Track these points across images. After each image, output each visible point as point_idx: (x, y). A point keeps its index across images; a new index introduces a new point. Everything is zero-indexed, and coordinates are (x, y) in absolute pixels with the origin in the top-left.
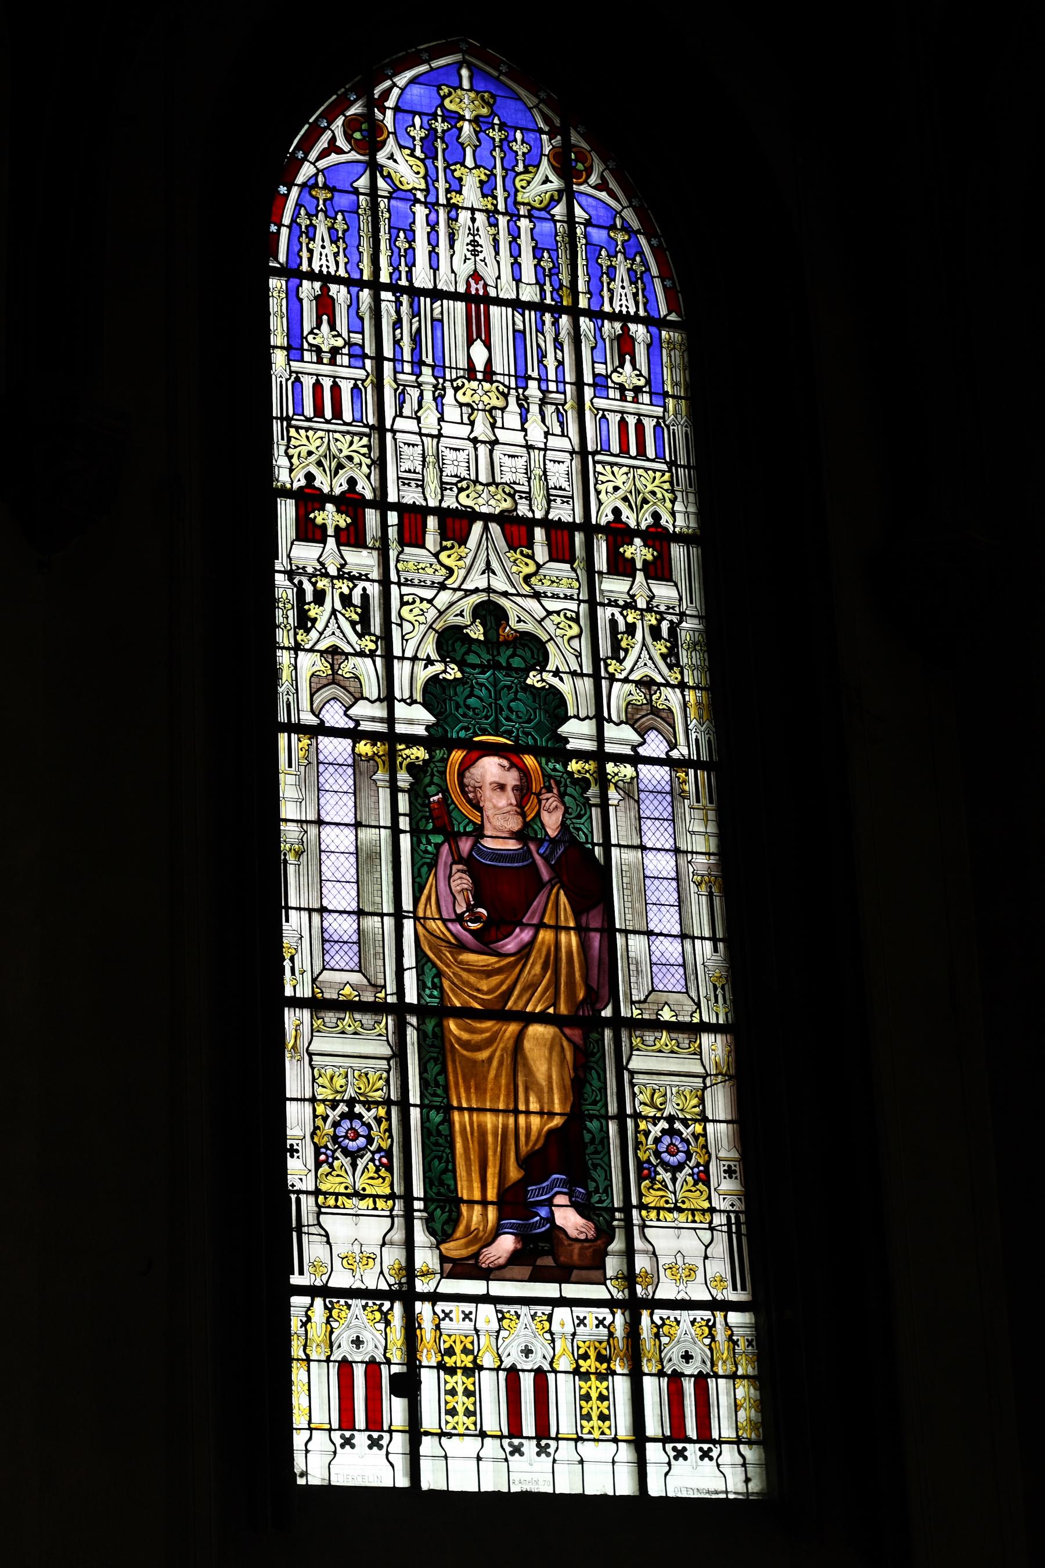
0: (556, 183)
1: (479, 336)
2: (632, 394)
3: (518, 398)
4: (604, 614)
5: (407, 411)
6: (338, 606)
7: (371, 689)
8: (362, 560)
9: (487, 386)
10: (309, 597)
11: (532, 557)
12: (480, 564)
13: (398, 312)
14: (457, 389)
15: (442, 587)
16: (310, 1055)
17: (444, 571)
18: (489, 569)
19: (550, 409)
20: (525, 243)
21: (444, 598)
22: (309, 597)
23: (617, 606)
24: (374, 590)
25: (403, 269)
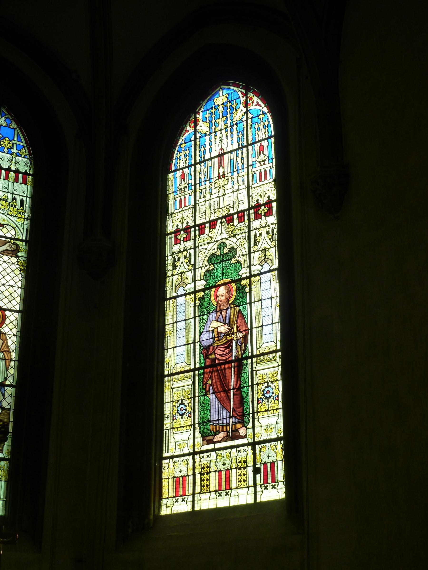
0: (244, 110)
1: (221, 166)
2: (263, 163)
3: (231, 179)
4: (252, 233)
5: (202, 196)
6: (183, 259)
7: (191, 280)
8: (190, 244)
9: (223, 179)
10: (177, 260)
11: (233, 225)
12: (220, 232)
13: (200, 169)
14: (215, 184)
15: (209, 243)
16: (172, 389)
17: (210, 238)
18: (222, 233)
19: (239, 179)
20: (235, 133)
21: (211, 245)
22: (177, 260)
23: (257, 229)
24: (192, 251)
25: (203, 156)
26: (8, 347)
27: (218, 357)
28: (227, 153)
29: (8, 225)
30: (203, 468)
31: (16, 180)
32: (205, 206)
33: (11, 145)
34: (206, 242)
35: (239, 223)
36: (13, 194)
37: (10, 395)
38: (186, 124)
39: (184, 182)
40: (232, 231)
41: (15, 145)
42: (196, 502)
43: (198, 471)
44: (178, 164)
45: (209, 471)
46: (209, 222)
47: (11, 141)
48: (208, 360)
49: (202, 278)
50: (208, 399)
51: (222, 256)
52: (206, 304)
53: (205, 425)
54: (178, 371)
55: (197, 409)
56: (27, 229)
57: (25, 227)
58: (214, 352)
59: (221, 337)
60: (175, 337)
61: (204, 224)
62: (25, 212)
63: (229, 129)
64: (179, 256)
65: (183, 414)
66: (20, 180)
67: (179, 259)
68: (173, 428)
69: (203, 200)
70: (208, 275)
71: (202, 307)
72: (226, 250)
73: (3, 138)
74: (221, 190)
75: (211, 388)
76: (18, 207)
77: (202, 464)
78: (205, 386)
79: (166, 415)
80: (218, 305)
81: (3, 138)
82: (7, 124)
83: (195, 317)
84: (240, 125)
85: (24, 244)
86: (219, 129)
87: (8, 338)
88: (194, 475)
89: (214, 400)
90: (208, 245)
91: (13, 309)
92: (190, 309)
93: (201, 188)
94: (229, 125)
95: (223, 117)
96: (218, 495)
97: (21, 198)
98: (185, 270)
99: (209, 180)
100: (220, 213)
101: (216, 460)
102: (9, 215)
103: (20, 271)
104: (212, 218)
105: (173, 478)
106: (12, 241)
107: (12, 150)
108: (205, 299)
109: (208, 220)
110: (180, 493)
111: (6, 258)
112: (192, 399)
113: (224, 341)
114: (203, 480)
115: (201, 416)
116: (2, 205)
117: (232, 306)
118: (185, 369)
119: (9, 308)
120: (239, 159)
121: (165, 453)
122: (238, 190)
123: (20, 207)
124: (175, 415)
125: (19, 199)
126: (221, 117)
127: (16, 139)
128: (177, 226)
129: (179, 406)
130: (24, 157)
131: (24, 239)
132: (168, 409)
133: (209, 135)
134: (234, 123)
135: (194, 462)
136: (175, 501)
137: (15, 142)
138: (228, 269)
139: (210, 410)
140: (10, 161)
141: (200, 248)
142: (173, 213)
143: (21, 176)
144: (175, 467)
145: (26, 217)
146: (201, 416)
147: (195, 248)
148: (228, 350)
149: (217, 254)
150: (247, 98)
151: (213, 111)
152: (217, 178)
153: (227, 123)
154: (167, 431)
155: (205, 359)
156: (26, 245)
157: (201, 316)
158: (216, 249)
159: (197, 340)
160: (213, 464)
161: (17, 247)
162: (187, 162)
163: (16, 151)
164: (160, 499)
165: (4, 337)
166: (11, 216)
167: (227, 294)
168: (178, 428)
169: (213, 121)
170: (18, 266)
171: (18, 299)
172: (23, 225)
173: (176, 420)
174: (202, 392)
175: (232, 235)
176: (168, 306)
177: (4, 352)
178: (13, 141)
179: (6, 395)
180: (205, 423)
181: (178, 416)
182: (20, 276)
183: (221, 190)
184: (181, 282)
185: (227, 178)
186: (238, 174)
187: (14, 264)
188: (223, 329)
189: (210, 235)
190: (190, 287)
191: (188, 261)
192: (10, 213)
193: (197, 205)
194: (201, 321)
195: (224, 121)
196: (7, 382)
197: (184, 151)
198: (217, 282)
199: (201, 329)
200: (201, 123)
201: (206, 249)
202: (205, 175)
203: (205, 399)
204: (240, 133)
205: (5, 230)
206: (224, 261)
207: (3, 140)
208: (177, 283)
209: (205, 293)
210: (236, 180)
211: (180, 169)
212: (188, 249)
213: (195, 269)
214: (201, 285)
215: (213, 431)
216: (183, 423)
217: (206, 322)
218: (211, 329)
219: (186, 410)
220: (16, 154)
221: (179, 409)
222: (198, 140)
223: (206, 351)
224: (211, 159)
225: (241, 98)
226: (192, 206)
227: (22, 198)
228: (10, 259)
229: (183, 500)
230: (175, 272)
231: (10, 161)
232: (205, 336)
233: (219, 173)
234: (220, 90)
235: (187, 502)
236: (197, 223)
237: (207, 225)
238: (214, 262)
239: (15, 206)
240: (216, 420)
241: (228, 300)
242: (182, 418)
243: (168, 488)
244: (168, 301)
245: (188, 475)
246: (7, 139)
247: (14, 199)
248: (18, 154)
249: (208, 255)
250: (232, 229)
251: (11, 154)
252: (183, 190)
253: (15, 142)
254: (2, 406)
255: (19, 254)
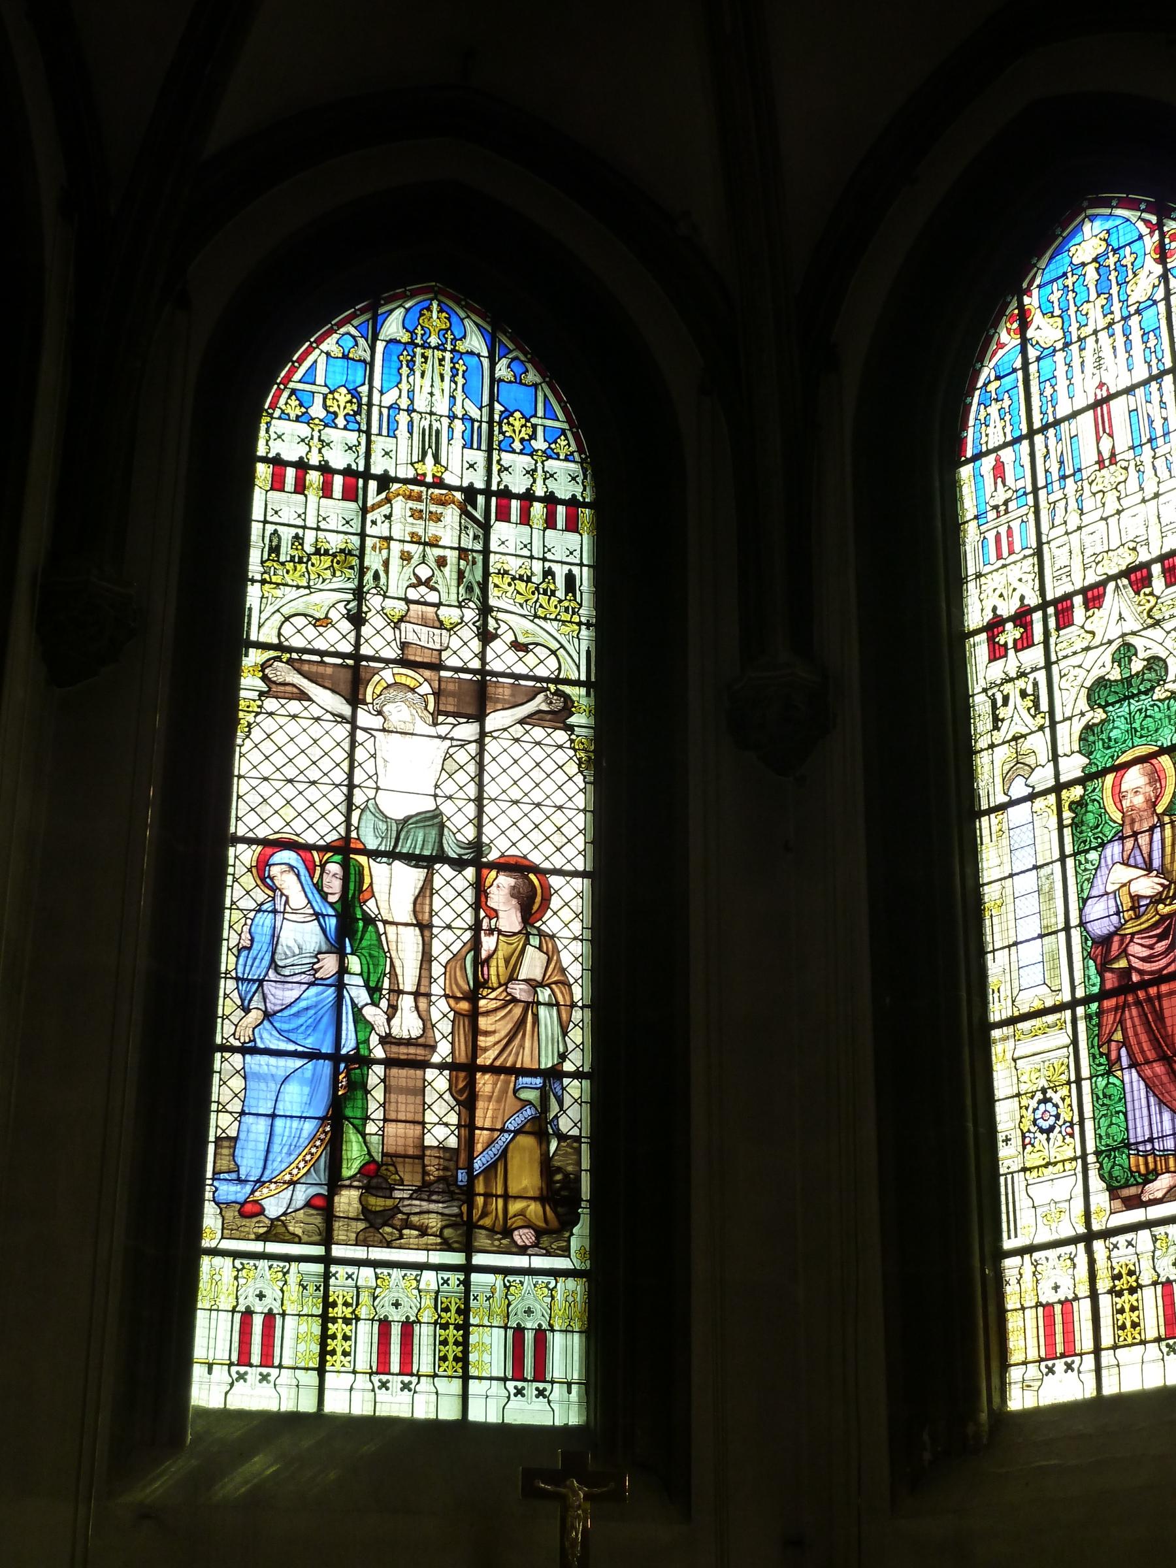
0: (1159, 269)
1: (1104, 431)
3: (1136, 466)
5: (1057, 521)
6: (1019, 699)
7: (1043, 755)
8: (1033, 656)
9: (1113, 468)
10: (1000, 702)
11: (1152, 594)
13: (1046, 446)
14: (1091, 484)
15: (1087, 649)
16: (1015, 1060)
17: (1089, 636)
20: (1136, 336)
21: (1093, 654)
22: (1000, 702)
24: (1041, 676)
25: (1050, 410)
26: (563, 971)
27: (1137, 964)
28: (1118, 394)
29: (537, 644)
30: (1118, 1277)
31: (550, 523)
32: (1067, 548)
33: (530, 431)
34: (1079, 646)
35: (1168, 585)
36: (544, 560)
37: (576, 1101)
38: (996, 325)
39: (1004, 485)
40: (1151, 610)
41: (540, 430)
42: (1104, 1372)
43: (1103, 1285)
44: (984, 439)
45: (1134, 1284)
46: (1084, 591)
47: (528, 420)
48: (1108, 975)
49: (1076, 748)
50: (1118, 1082)
51: (1127, 681)
52: (1090, 819)
53: (1115, 1157)
54: (1026, 1010)
55: (1088, 1113)
56: (588, 652)
57: (584, 647)
58: (1124, 953)
59: (1142, 909)
60: (1011, 916)
61: (1068, 597)
62: (581, 605)
63: (1118, 328)
64: (1005, 693)
65: (1051, 1129)
66: (561, 521)
67: (1006, 699)
68: (1024, 1170)
69: (1061, 530)
70: (1091, 738)
71: (1082, 830)
72: (1137, 665)
73: (506, 414)
74: (1111, 497)
75: (1123, 1051)
76: (560, 594)
77: (1114, 1265)
78: (1105, 1046)
79: (1004, 1134)
80: (1127, 821)
81: (506, 414)
82: (515, 376)
83: (1063, 858)
84: (1149, 314)
85: (583, 691)
86: (1088, 330)
87: (560, 947)
88: (1094, 1296)
89: (1135, 1084)
90: (1082, 656)
91: (568, 867)
92: (1047, 838)
93: (1052, 498)
94: (1118, 318)
95: (1099, 296)
96: (1165, 1350)
97: (566, 568)
98: (1025, 731)
99: (1073, 475)
100: (1113, 564)
101: (1154, 1252)
102: (539, 618)
103: (579, 766)
104: (1092, 579)
105: (1036, 1307)
106: (552, 687)
107: (533, 442)
108: (1087, 805)
109: (1078, 586)
110: (1060, 1349)
111: (538, 733)
112: (1074, 1086)
113: (1150, 919)
114: (1121, 1311)
115: (1102, 1132)
116: (518, 593)
117: (1167, 819)
118: (1047, 1005)
119: (558, 867)
120: (1155, 411)
121: (1009, 1238)
122: (1157, 495)
123: (566, 595)
124: (1029, 1131)
125: (560, 572)
126: (1093, 295)
127: (540, 413)
128: (995, 609)
129: (1037, 1108)
130: (566, 459)
131: (583, 678)
132: (1006, 1115)
133: (1062, 350)
134: (1132, 309)
135: (1092, 1262)
136: (1045, 1371)
137: (539, 421)
138: (1146, 716)
139: (1125, 1114)
140: (532, 473)
141: (1063, 664)
142: (979, 576)
143: (561, 510)
144: (1039, 1277)
145: (584, 620)
146: (1102, 1132)
147: (1048, 665)
148: (1164, 943)
149: (1112, 678)
150: (1162, 235)
151: (1069, 282)
152: (1097, 467)
153: (1112, 313)
154: (1009, 1177)
155: (1100, 973)
156: (588, 694)
157: (1079, 853)
158: (1109, 665)
159: (1074, 921)
160: (1146, 1264)
161: (565, 702)
162: (1008, 429)
163: (544, 446)
164: (1005, 1366)
165: (550, 946)
166: (545, 619)
167: (1149, 789)
168: (1038, 1167)
169: (1073, 309)
170: (571, 753)
171: (580, 842)
172: (576, 640)
173: (1033, 1146)
174: (1100, 1065)
175: (1150, 621)
176: (986, 832)
177: (553, 986)
178: (534, 420)
179: (568, 1101)
180: (1114, 1149)
181: (1038, 1134)
182: (579, 779)
183: (1111, 497)
184: (1018, 763)
185: (1124, 464)
186: (1153, 450)
187: (560, 747)
188: (1147, 886)
189: (1088, 627)
190: (1043, 778)
191: (1031, 704)
192: (540, 612)
193: (1045, 547)
194: (1082, 867)
195: (1103, 307)
196: (568, 1067)
197: (997, 400)
198: (1118, 757)
199: (1082, 891)
200: (1037, 319)
201: (1080, 666)
202: (1061, 463)
203: (1108, 1083)
204: (1152, 334)
205: (530, 659)
206: (1133, 696)
207: (507, 418)
208: (1007, 767)
209: (1085, 790)
210: (1148, 468)
211: (989, 452)
212: (1028, 670)
213: (1053, 724)
214: (1072, 767)
215: (1139, 1172)
216: (1053, 1154)
217: (1096, 869)
218: (1110, 888)
219: (1057, 1117)
220: (544, 452)
221: (1038, 1114)
222: (1033, 368)
223: (1102, 949)
224: (1074, 415)
225: (1147, 239)
226: (1031, 551)
227: (570, 571)
228: (549, 735)
229: (1069, 1367)
230: (998, 737)
231: (532, 473)
232: (1097, 909)
233: (1099, 453)
234: (1083, 221)
235: (1079, 1372)
236: (1049, 597)
237: (1078, 600)
238: (1106, 701)
239: (553, 593)
240: (1144, 1142)
241: (1154, 805)
242: (1048, 1140)
243: (1023, 1336)
244: (985, 820)
245: (1076, 1298)
246: (518, 415)
247: (548, 573)
248: (549, 452)
249: (1088, 684)
250: (1148, 606)
251: (531, 455)
252: (1002, 508)
253: (539, 421)
254: (559, 1129)
255: (573, 720)
